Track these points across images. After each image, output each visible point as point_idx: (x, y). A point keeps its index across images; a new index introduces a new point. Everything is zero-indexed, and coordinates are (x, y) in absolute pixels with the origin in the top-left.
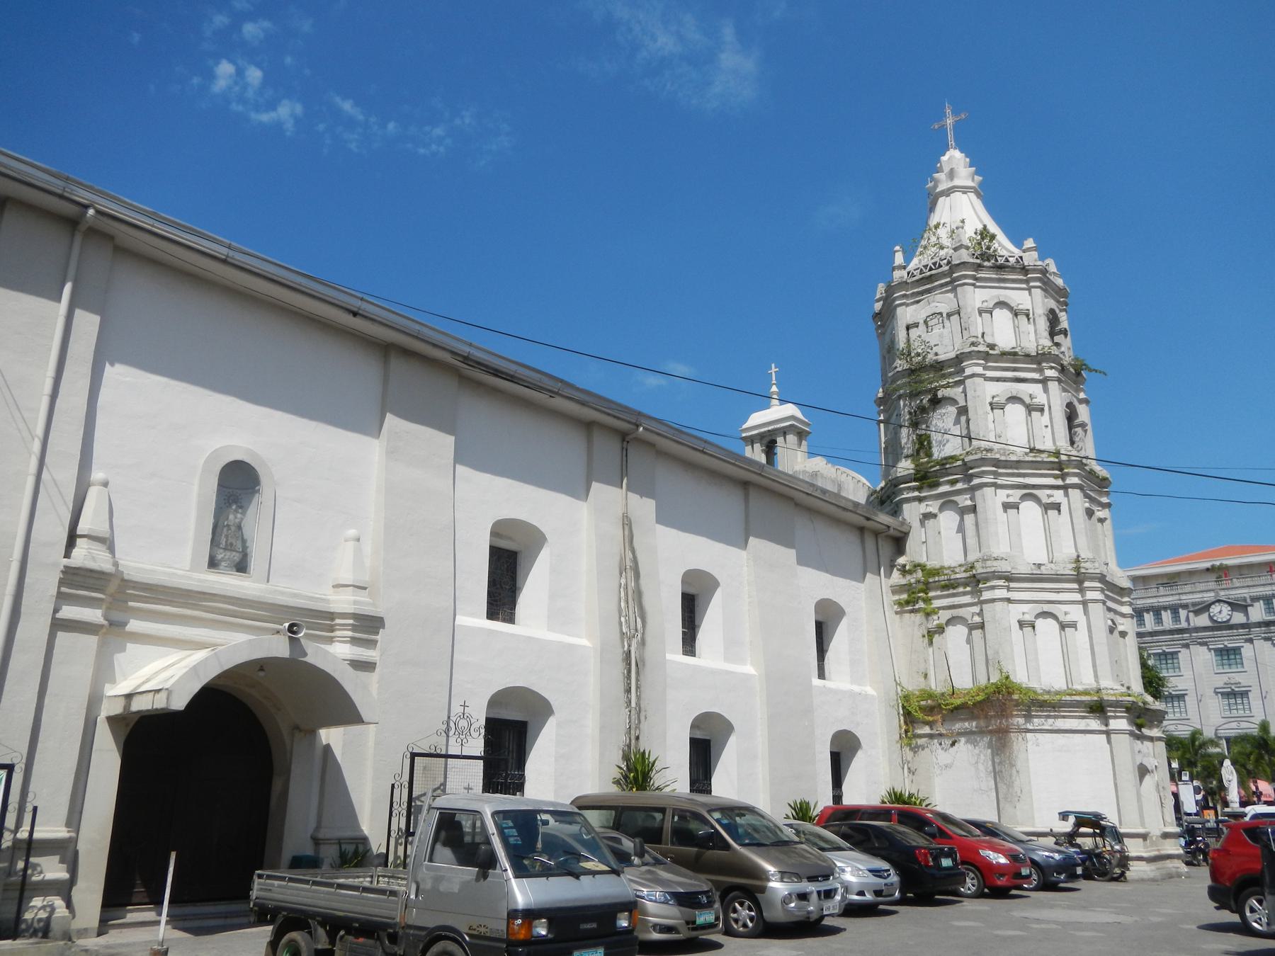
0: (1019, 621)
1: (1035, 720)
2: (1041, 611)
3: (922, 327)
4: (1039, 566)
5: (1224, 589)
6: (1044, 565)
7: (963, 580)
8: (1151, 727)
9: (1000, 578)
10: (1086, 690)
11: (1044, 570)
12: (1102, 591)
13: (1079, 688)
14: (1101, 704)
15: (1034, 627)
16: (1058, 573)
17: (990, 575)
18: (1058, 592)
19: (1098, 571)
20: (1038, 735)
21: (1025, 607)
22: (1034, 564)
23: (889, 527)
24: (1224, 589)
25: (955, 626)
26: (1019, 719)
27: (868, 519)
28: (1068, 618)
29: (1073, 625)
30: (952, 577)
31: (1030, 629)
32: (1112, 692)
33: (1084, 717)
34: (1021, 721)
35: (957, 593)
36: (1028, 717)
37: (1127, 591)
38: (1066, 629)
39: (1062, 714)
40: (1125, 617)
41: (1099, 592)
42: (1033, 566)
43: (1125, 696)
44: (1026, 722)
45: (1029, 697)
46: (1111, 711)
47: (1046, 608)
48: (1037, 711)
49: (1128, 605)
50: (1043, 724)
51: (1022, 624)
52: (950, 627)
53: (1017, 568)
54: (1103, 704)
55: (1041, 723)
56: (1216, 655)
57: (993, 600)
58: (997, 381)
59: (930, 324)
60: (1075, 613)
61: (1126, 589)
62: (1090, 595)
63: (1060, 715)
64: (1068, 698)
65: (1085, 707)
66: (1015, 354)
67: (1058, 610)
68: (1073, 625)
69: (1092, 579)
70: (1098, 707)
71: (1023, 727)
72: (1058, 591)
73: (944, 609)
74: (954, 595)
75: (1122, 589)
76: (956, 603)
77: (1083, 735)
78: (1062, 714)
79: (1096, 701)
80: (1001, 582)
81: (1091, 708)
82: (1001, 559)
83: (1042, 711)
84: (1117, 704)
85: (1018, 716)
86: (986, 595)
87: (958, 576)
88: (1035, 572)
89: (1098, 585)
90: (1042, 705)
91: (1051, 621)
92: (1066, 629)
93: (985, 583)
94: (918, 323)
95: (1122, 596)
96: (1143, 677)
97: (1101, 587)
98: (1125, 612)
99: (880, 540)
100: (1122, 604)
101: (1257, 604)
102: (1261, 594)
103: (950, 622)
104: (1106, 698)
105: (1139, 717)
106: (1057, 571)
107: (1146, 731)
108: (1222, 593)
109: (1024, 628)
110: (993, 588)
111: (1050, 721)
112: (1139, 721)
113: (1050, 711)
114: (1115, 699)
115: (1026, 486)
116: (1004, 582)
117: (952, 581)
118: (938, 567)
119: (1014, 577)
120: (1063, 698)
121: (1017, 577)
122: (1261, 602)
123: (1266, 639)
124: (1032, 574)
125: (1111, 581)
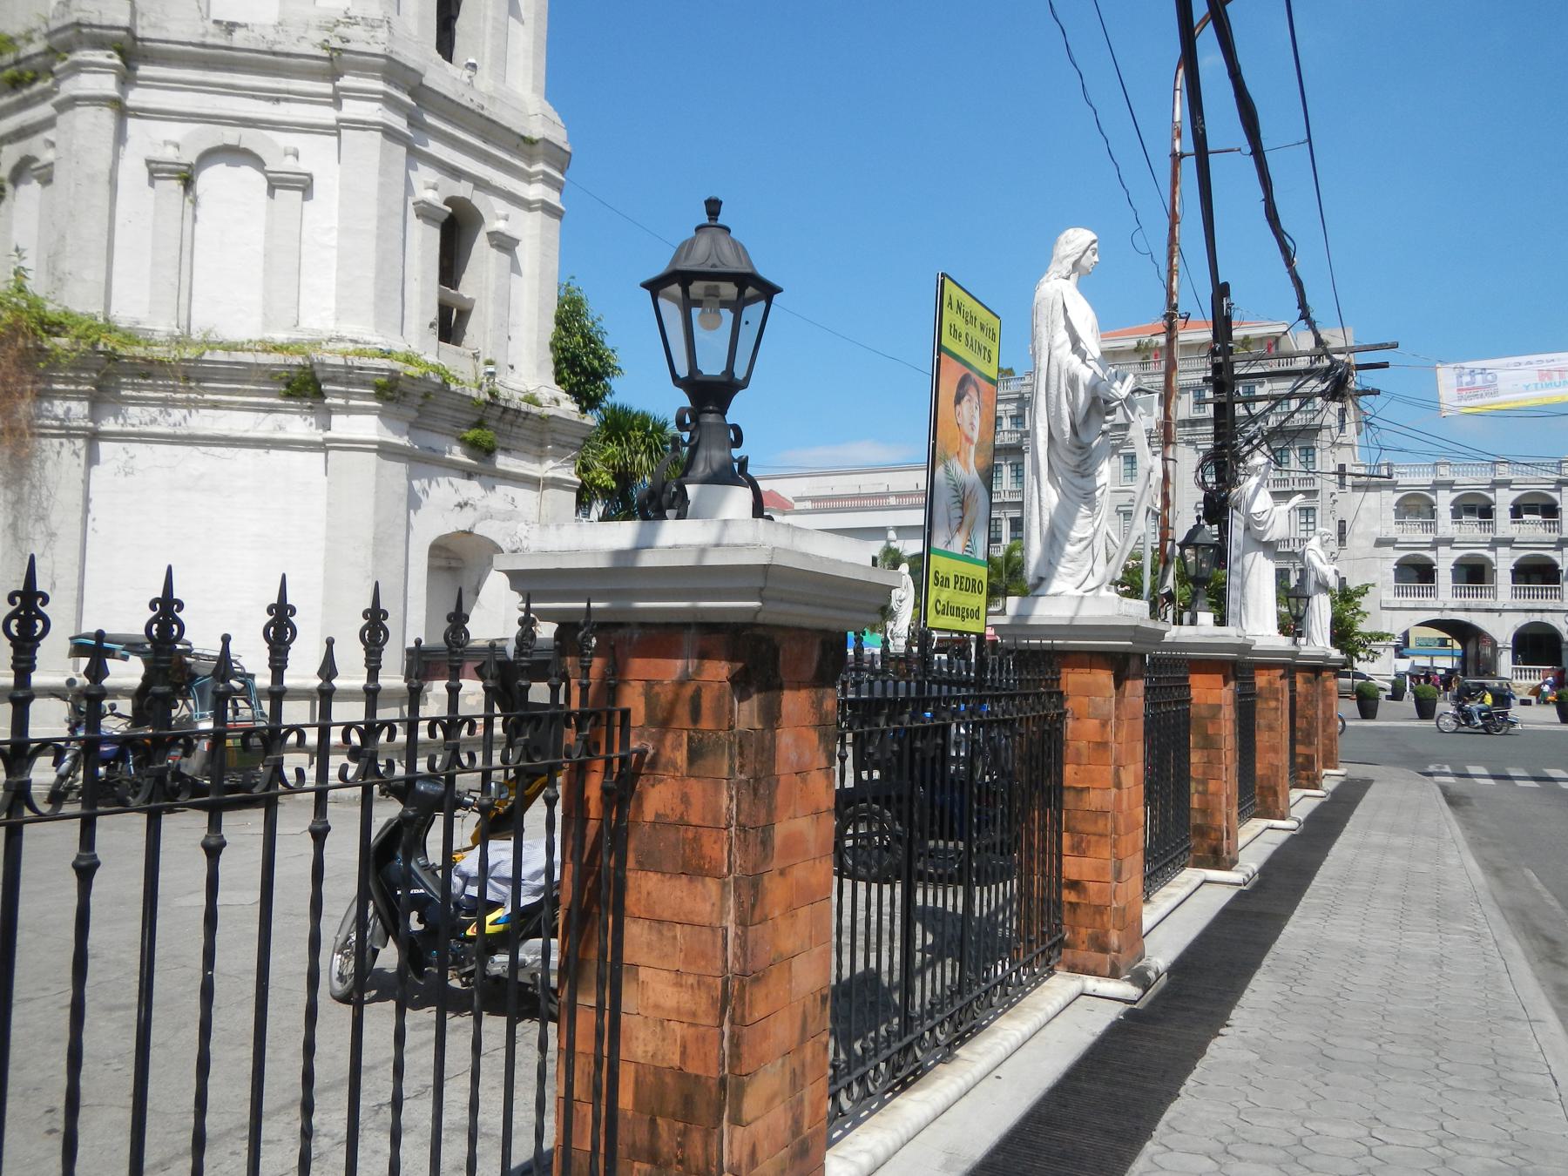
0: (149, 162)
1: (133, 410)
2: (220, 144)
4: (231, 27)
5: (1147, 374)
6: (246, 26)
7: (40, 59)
8: (540, 458)
9: (99, 43)
10: (296, 342)
11: (239, 39)
12: (389, 101)
13: (280, 337)
14: (313, 374)
15: (188, 182)
16: (277, 48)
17: (70, 33)
18: (278, 100)
19: (378, 49)
20: (136, 449)
21: (176, 130)
22: (216, 22)
24: (1147, 374)
25: (28, 183)
26: (74, 405)
28: (289, 164)
29: (304, 185)
30: (22, 54)
31: (176, 186)
32: (341, 346)
33: (271, 409)
34: (79, 409)
35: (32, 96)
36: (103, 396)
37: (540, 147)
38: (278, 191)
39: (208, 397)
40: (531, 210)
41: (378, 105)
42: (212, 28)
43: (374, 356)
44: (93, 416)
45: (94, 345)
46: (335, 394)
47: (230, 136)
48: (139, 387)
49: (542, 181)
50: (154, 421)
51: (155, 170)
52: (23, 188)
53: (162, 28)
54: (320, 376)
55: (147, 419)
56: (1126, 463)
57: (73, 102)
60: (315, 155)
61: (537, 141)
62: (353, 109)
63: (206, 401)
64: (220, 356)
65: (272, 383)
67: (274, 147)
68: (304, 185)
69: (363, 65)
70: (308, 383)
71: (75, 424)
72: (276, 97)
73: (10, 142)
74: (26, 104)
75: (531, 142)
76: (25, 124)
77: (261, 452)
78: (208, 397)
79: (299, 366)
80: (100, 56)
81: (288, 385)
83: (154, 388)
84: (349, 377)
85: (65, 396)
86: (70, 87)
87: (32, 49)
88: (209, 40)
89: (380, 86)
90: (149, 370)
91: (248, 175)
92: (278, 191)
93: (65, 59)
95: (531, 160)
96: (552, 346)
97: (385, 93)
98: (531, 198)
100: (528, 178)
101: (1185, 396)
102: (1192, 382)
103: (22, 171)
104: (317, 356)
105: (479, 424)
106: (275, 42)
107: (503, 462)
108: (1145, 380)
109: (158, 183)
110: (77, 68)
111: (177, 414)
112: (486, 435)
113: (174, 389)
114: (341, 362)
116: (110, 57)
117: (22, 66)
118: (11, 34)
119: (152, 50)
120: (207, 356)
121: (161, 51)
122: (1191, 393)
123: (1189, 443)
124: (203, 45)
125: (471, 105)
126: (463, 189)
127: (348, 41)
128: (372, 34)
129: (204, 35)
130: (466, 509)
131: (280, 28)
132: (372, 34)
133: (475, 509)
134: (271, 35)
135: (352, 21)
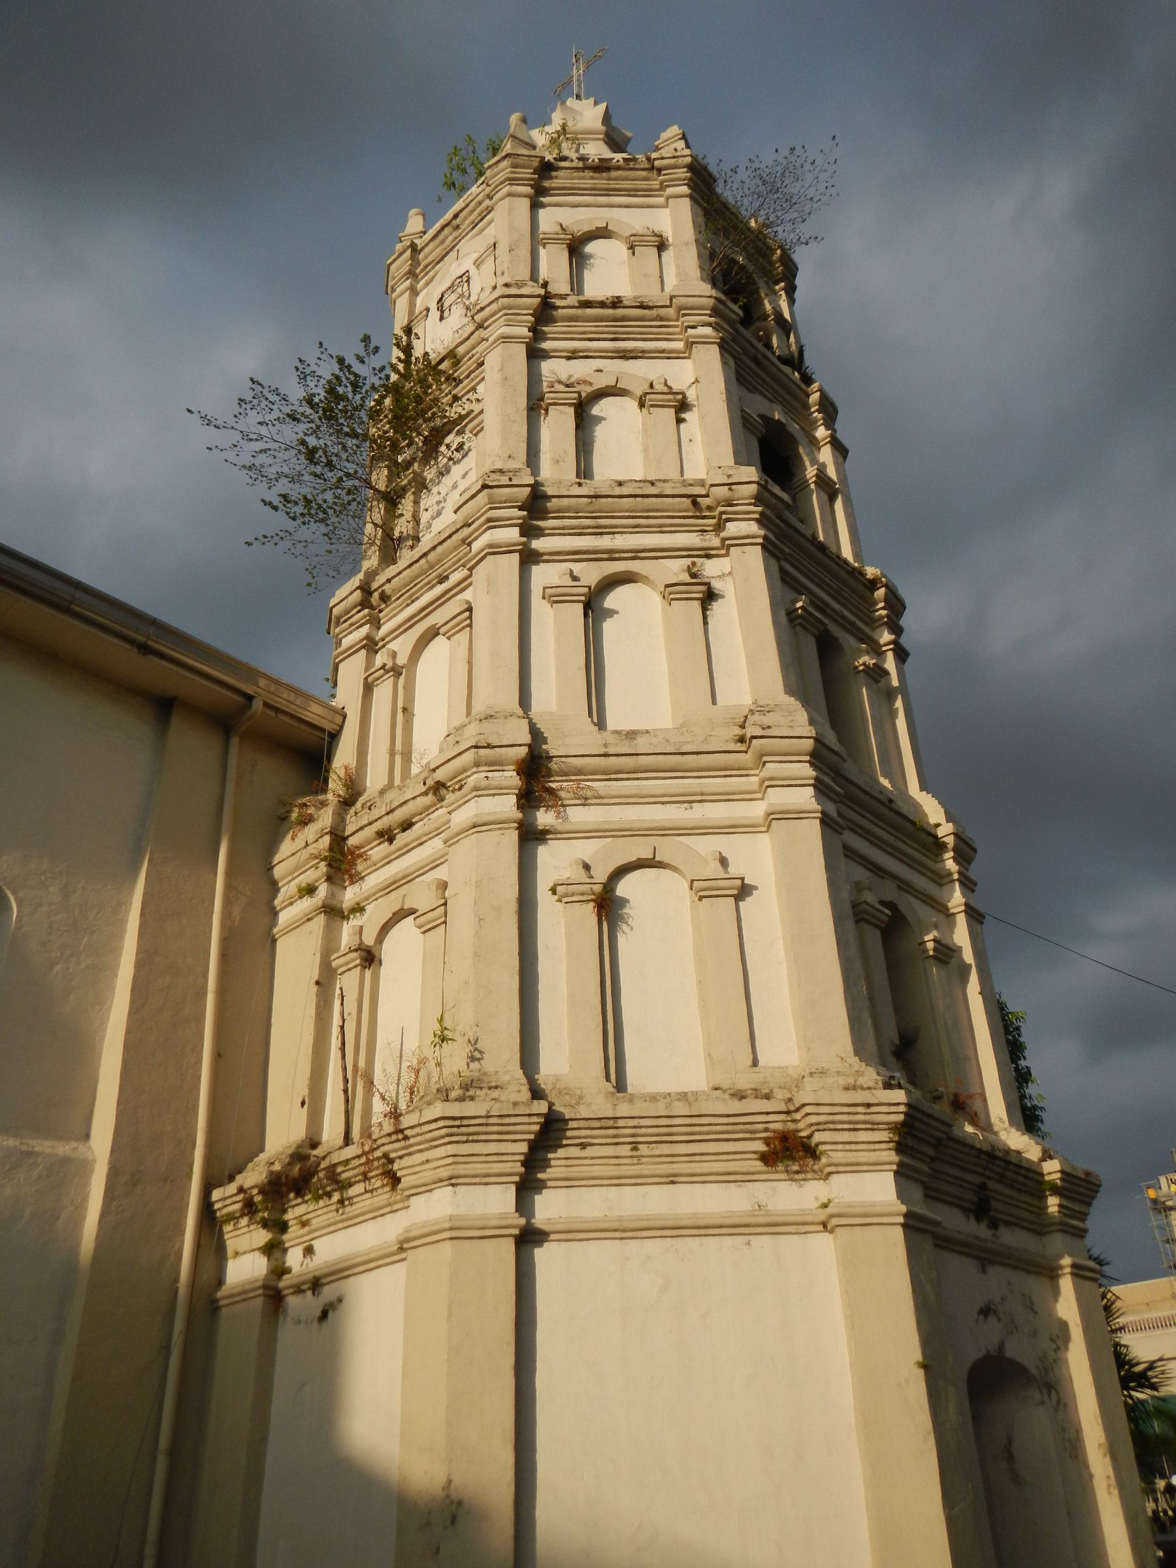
3: (434, 314)
6: (647, 732)
11: (642, 745)
22: (617, 732)
23: (250, 698)
27: (145, 649)
42: (611, 739)
58: (569, 358)
59: (446, 305)
66: (616, 303)
72: (689, 800)
82: (506, 717)
94: (428, 310)
99: (235, 742)
106: (682, 744)
115: (612, 555)
126: (890, 892)
127: (769, 727)
128: (791, 718)
129: (606, 745)
130: (992, 1320)
131: (684, 729)
132: (791, 718)
133: (999, 1319)
134: (675, 738)
135: (767, 709)
